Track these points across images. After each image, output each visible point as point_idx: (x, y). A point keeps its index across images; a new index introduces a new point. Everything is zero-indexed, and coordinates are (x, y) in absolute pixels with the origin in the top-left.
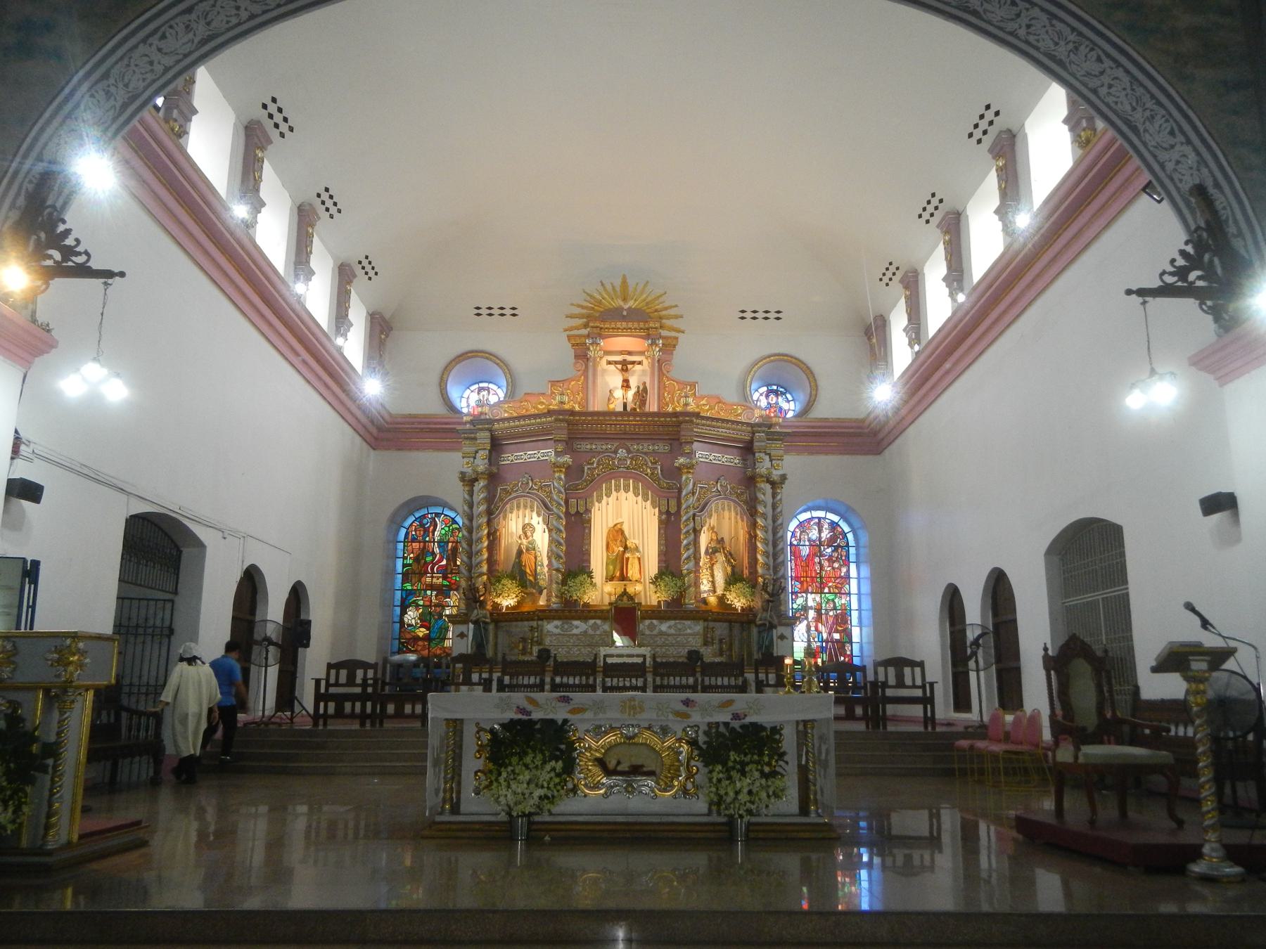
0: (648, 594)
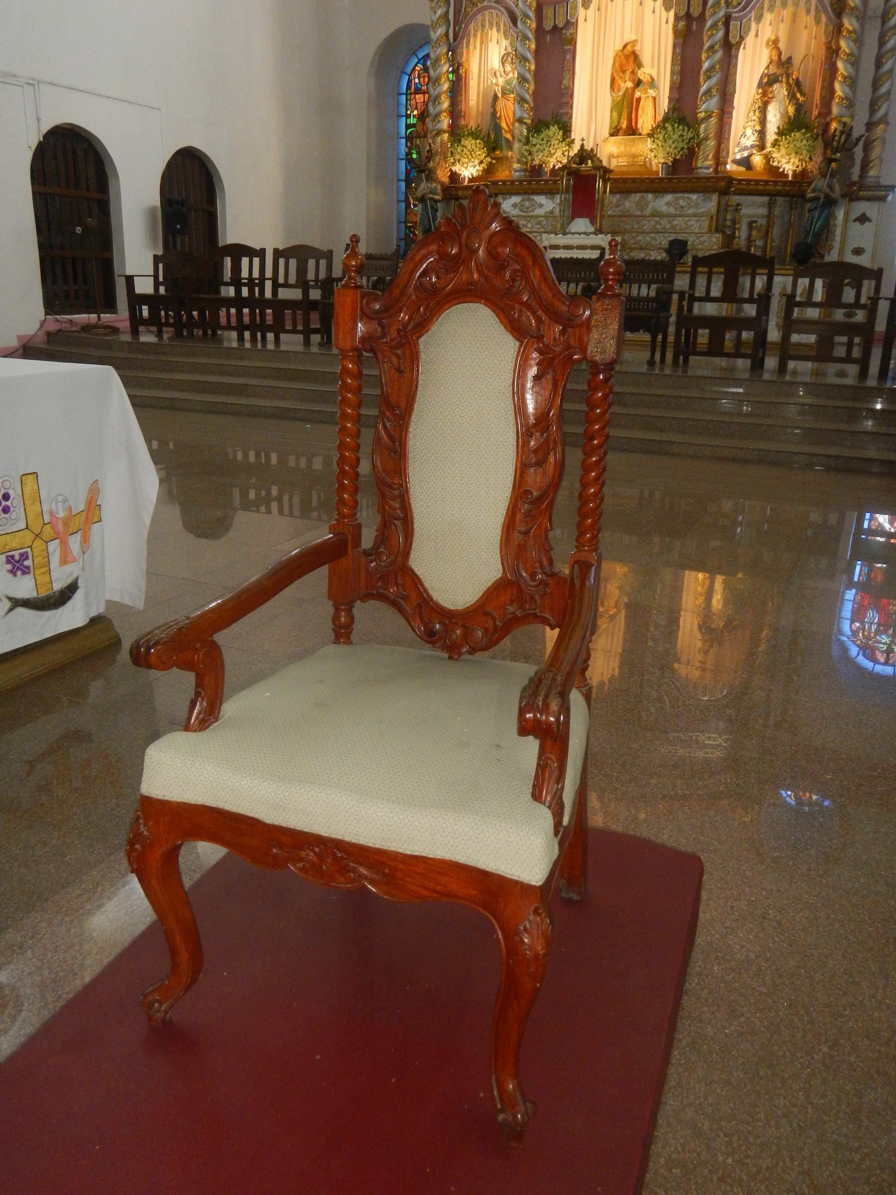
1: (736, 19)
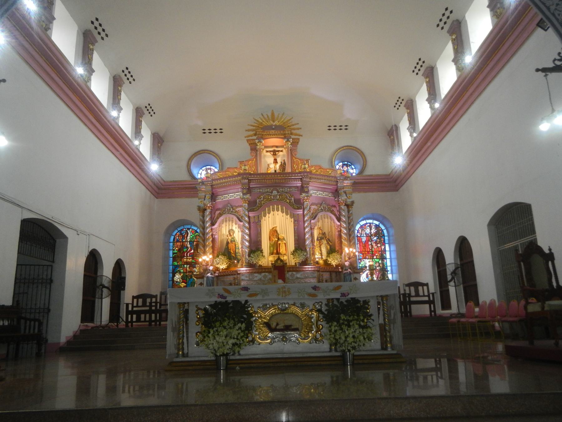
0: (290, 259)
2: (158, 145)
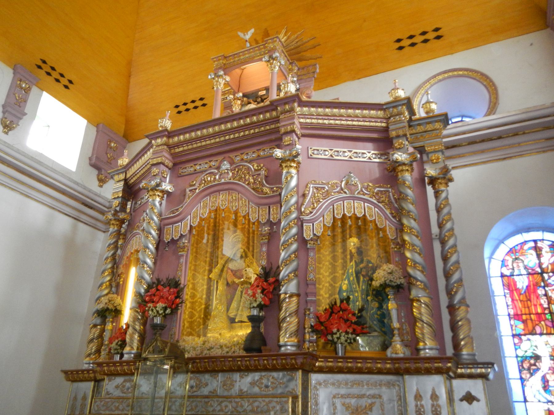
1: (308, 221)
2: (110, 145)
